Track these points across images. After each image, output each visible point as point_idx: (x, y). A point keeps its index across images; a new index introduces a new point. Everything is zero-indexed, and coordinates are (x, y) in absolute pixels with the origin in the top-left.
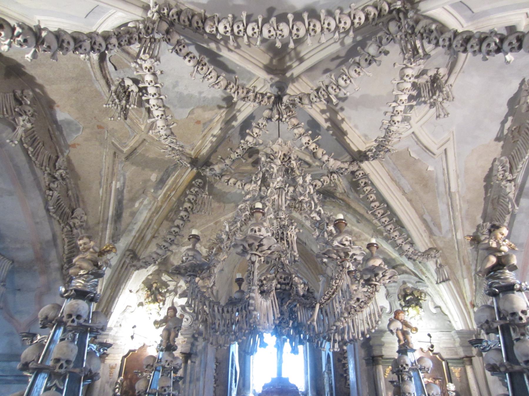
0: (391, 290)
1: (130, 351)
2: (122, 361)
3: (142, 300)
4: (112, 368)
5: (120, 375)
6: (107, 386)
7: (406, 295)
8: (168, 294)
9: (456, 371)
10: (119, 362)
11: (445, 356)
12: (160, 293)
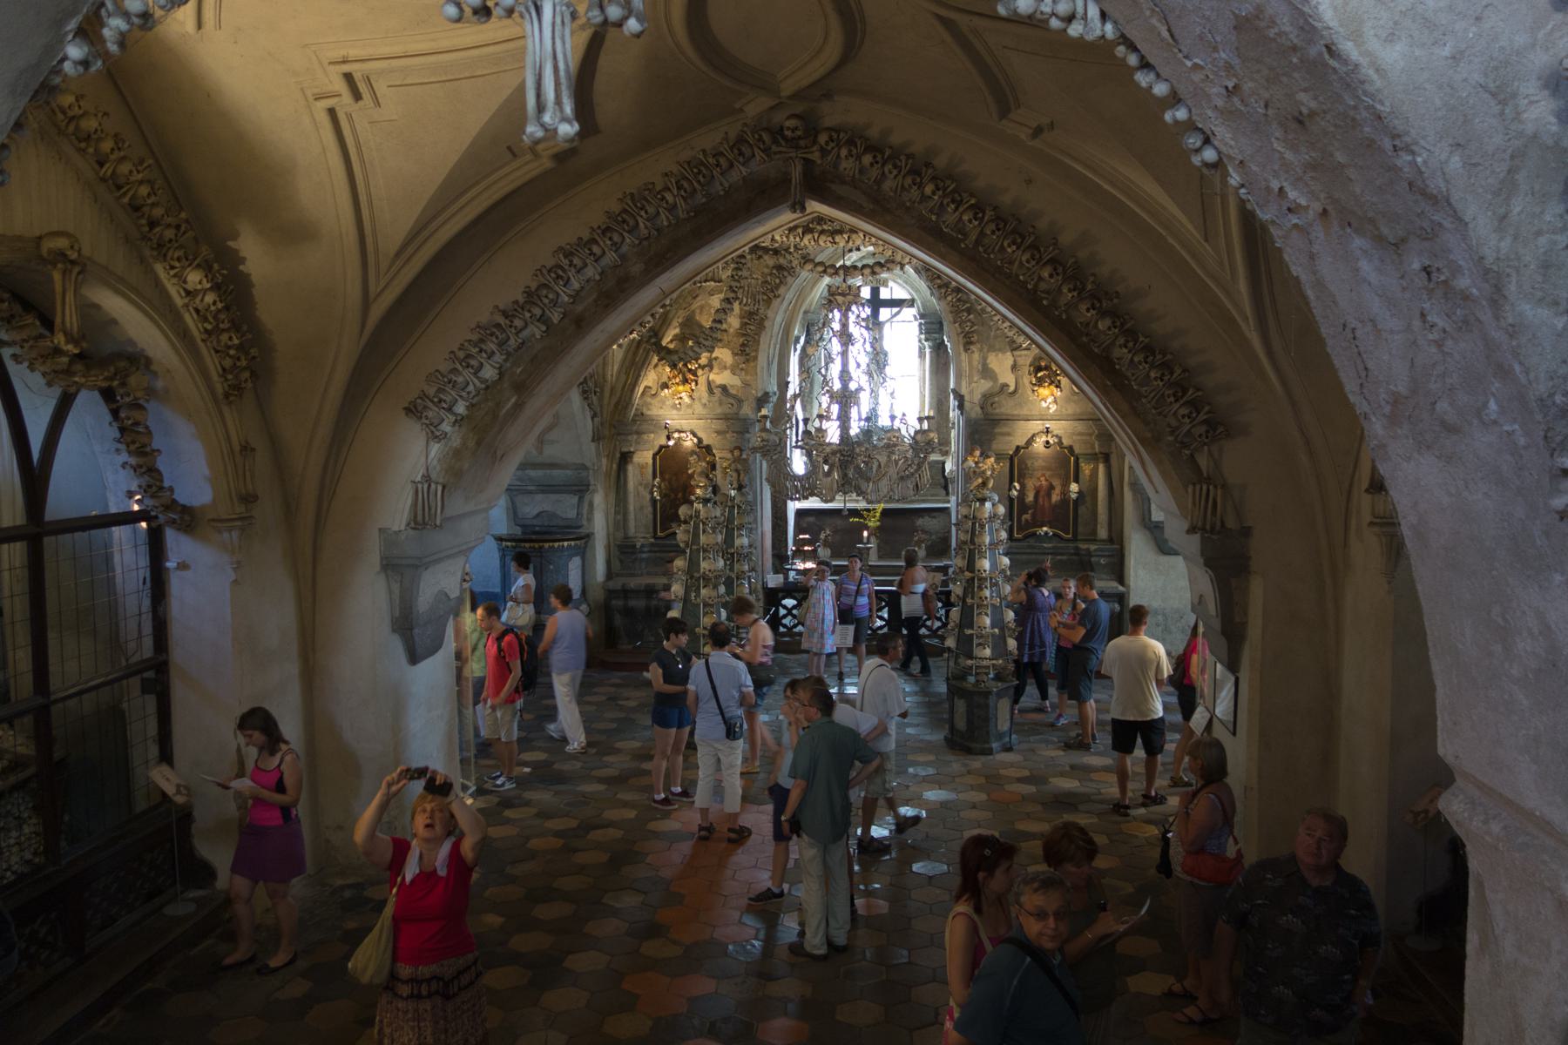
0: (1021, 361)
1: (661, 447)
2: (654, 458)
3: (665, 379)
4: (642, 467)
5: (654, 477)
6: (641, 489)
7: (1039, 369)
8: (700, 372)
9: (1086, 469)
10: (650, 461)
11: (1077, 450)
12: (690, 370)
